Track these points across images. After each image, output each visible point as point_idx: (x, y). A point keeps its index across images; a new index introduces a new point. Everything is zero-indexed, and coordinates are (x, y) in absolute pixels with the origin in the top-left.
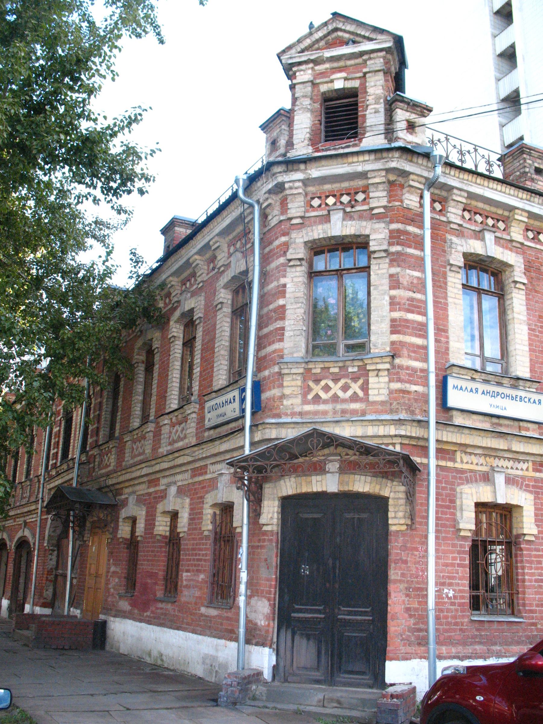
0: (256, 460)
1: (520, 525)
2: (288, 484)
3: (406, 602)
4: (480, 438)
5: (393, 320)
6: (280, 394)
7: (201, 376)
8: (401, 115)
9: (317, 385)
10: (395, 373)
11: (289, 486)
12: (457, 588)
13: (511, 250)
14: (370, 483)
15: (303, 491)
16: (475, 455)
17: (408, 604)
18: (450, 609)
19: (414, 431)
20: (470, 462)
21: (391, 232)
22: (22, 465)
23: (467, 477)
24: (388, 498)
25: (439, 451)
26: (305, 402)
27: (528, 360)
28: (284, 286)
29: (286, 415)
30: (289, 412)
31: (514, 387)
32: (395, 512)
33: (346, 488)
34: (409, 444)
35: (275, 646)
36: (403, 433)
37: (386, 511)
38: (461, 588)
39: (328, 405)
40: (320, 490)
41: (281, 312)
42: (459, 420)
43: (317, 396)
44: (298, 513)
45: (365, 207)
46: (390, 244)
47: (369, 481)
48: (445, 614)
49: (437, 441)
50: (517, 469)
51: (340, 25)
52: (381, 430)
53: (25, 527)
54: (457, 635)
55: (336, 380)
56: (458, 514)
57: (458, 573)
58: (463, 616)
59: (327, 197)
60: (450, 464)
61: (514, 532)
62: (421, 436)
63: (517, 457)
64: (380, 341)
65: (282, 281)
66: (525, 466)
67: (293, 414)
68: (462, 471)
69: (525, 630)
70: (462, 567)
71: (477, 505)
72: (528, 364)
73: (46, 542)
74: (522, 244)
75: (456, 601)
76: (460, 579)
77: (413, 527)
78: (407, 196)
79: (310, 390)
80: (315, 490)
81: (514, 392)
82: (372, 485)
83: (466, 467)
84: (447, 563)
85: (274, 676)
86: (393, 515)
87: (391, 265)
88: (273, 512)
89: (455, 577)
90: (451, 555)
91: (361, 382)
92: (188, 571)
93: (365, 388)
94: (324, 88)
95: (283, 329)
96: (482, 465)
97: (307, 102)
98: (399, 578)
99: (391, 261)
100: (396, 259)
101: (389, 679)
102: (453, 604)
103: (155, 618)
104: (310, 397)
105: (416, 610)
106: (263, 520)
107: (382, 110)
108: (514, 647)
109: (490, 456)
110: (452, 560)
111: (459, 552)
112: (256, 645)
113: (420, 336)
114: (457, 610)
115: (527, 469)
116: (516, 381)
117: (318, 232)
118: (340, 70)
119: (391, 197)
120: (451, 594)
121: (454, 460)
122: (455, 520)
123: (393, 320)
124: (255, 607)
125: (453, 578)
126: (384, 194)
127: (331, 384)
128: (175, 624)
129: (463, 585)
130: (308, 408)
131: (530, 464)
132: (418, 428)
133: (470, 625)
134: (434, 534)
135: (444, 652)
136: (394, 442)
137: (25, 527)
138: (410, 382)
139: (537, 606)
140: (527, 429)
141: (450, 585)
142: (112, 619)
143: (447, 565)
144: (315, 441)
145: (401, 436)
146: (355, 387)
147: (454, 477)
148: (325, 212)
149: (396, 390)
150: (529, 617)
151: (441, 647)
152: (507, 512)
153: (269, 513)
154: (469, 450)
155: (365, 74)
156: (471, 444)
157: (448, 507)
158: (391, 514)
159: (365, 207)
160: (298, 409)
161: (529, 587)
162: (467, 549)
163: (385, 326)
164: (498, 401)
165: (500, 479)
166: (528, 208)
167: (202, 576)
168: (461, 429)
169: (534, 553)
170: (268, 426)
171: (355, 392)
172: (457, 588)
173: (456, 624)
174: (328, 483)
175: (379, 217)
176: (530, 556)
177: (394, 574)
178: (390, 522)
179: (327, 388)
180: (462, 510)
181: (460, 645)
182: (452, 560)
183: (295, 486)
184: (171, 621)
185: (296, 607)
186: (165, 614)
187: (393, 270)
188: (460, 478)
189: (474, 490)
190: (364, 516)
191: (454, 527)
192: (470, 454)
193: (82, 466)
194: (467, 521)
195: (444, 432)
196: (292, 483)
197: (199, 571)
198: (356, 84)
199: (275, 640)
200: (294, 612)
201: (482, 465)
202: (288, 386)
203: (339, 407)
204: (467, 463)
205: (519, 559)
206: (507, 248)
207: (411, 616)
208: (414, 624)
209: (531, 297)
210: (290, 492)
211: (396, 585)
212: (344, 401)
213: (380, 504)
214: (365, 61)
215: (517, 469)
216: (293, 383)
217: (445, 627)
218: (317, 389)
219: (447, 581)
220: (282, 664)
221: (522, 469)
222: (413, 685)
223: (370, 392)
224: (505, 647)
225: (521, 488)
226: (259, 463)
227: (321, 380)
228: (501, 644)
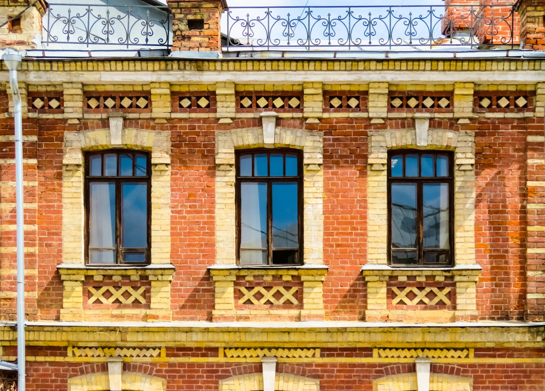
13: (153, 128)
20: (84, 354)
27: (169, 244)
50: (145, 356)
66: (155, 353)
68: (79, 364)
72: (169, 249)
74: (169, 120)
83: (77, 360)
96: (99, 356)
147: (67, 370)
192: (85, 348)
201: (99, 356)
204: (81, 356)
206: (147, 127)
209: (178, 176)
221: (151, 356)
225: (150, 374)
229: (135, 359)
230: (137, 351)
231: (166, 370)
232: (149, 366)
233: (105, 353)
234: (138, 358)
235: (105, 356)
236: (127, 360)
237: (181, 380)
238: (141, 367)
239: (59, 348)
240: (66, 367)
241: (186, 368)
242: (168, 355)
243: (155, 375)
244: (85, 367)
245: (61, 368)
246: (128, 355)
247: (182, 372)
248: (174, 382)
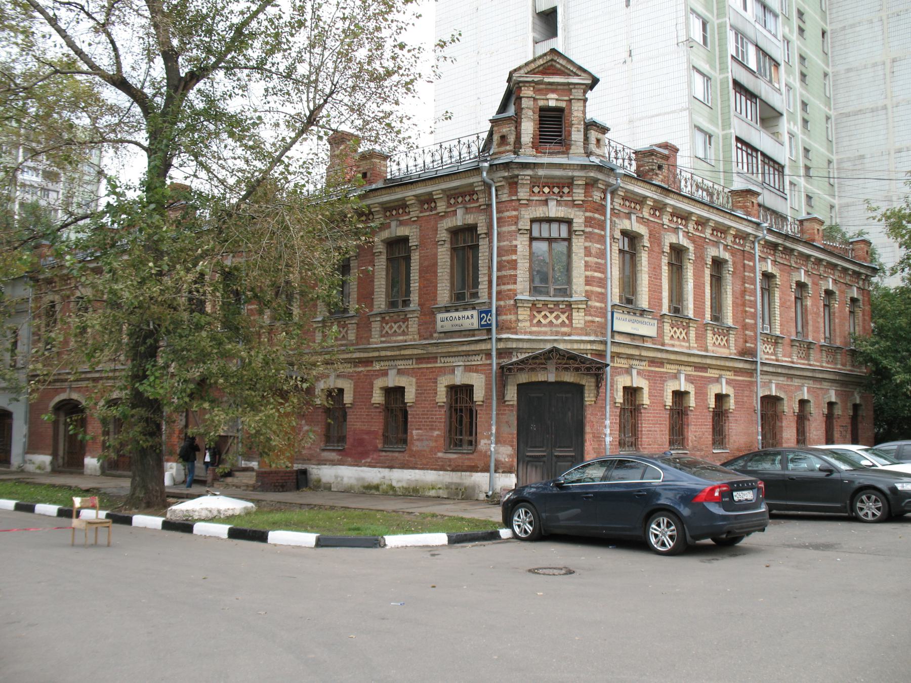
5: (586, 277)
7: (420, 289)
8: (593, 135)
10: (587, 311)
11: (523, 378)
21: (586, 218)
26: (532, 325)
28: (516, 246)
29: (521, 333)
31: (641, 315)
33: (559, 379)
41: (514, 265)
45: (570, 199)
46: (586, 226)
51: (556, 58)
52: (582, 346)
55: (551, 313)
59: (544, 187)
61: (637, 403)
63: (641, 359)
64: (579, 290)
65: (514, 243)
67: (525, 333)
71: (624, 388)
78: (595, 193)
79: (535, 317)
81: (640, 319)
87: (586, 241)
91: (566, 314)
92: (417, 429)
93: (570, 318)
94: (541, 103)
95: (516, 276)
97: (530, 113)
99: (586, 237)
100: (589, 236)
104: (535, 321)
106: (506, 399)
107: (582, 130)
113: (600, 287)
116: (643, 312)
117: (540, 212)
118: (553, 91)
119: (587, 194)
123: (586, 277)
126: (583, 191)
127: (548, 314)
128: (404, 466)
130: (535, 329)
138: (595, 316)
146: (563, 317)
148: (543, 198)
155: (570, 100)
158: (586, 395)
159: (570, 199)
160: (528, 330)
163: (582, 280)
164: (636, 325)
166: (655, 197)
167: (436, 433)
175: (578, 206)
177: (588, 429)
187: (587, 244)
190: (569, 395)
197: (432, 429)
198: (563, 104)
203: (554, 329)
210: (524, 381)
212: (556, 326)
213: (579, 389)
214: (571, 90)
218: (539, 317)
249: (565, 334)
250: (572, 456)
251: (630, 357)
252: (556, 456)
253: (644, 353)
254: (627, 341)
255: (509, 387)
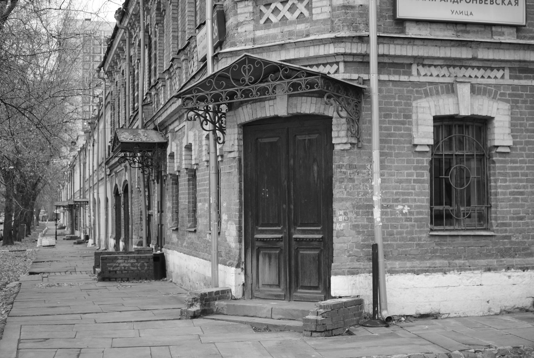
0: (199, 91)
1: (493, 138)
2: (245, 110)
3: (353, 220)
4: (437, 48)
6: (236, 23)
9: (268, 9)
11: (246, 114)
12: (413, 204)
14: (316, 104)
15: (258, 117)
16: (435, 66)
17: (356, 221)
18: (405, 225)
19: (357, 48)
20: (429, 74)
22: (122, 110)
23: (425, 91)
24: (331, 118)
25: (381, 66)
26: (256, 28)
30: (242, 39)
32: (338, 131)
33: (294, 111)
34: (353, 62)
35: (243, 267)
36: (342, 51)
37: (331, 130)
38: (418, 204)
39: (276, 29)
40: (272, 114)
42: (412, 31)
43: (268, 19)
44: (257, 139)
47: (315, 102)
48: (399, 230)
49: (379, 56)
50: (489, 77)
53: (126, 171)
54: (414, 250)
56: (414, 129)
57: (414, 189)
58: (421, 232)
60: (404, 78)
61: (489, 144)
62: (363, 52)
63: (488, 65)
66: (499, 74)
67: (245, 42)
69: (496, 244)
70: (419, 183)
71: (436, 119)
73: (137, 183)
75: (412, 217)
76: (417, 195)
77: (360, 145)
80: (268, 115)
82: (318, 106)
83: (423, 79)
84: (401, 180)
85: (243, 295)
86: (336, 135)
88: (235, 139)
89: (411, 193)
90: (406, 171)
98: (345, 196)
101: (334, 292)
102: (407, 220)
103: (188, 248)
104: (262, 22)
105: (364, 226)
108: (482, 261)
109: (454, 67)
110: (407, 176)
111: (415, 168)
112: (229, 266)
114: (413, 226)
115: (503, 77)
120: (406, 210)
121: (410, 74)
122: (411, 136)
124: (231, 231)
125: (409, 194)
127: (280, 6)
129: (422, 201)
130: (259, 33)
131: (507, 72)
132: (359, 44)
133: (429, 239)
134: (378, 151)
135: (398, 266)
136: (337, 60)
137: (126, 171)
139: (512, 218)
140: (502, 34)
141: (405, 201)
142: (168, 250)
143: (401, 182)
144: (247, 67)
145: (344, 54)
149: (338, 7)
150: (501, 230)
151: (394, 262)
152: (483, 124)
153: (230, 140)
154: (426, 62)
156: (426, 55)
157: (403, 123)
158: (334, 134)
160: (251, 36)
161: (502, 201)
162: (426, 164)
165: (464, 90)
168: (412, 41)
169: (509, 165)
170: (223, 55)
171: (301, 13)
172: (413, 204)
173: (412, 239)
174: (278, 107)
176: (504, 168)
177: (337, 192)
178: (333, 142)
179: (276, 11)
180: (417, 125)
181: (417, 259)
182: (407, 176)
183: (251, 112)
184: (195, 249)
185: (260, 228)
186: (193, 243)
188: (417, 92)
189: (432, 104)
190: (314, 137)
191: (410, 142)
192: (430, 66)
193: (145, 107)
194: (424, 134)
195: (392, 46)
196: (248, 109)
199: (243, 260)
200: (258, 233)
202: (241, 14)
203: (286, 29)
204: (425, 75)
205: (492, 172)
207: (359, 233)
208: (363, 241)
211: (341, 204)
212: (292, 23)
215: (489, 77)
216: (247, 10)
217: (399, 242)
218: (268, 13)
219: (401, 197)
220: (250, 282)
221: (496, 77)
222: (361, 298)
223: (314, 11)
224: (471, 261)
226: (201, 94)
227: (271, 4)
228: (466, 258)
229: (480, 81)
230: (482, 72)
231: (509, 94)
232: (493, 88)
233: (450, 73)
234: (482, 79)
235: (449, 76)
236: (474, 81)
237: (524, 105)
238: (485, 90)
239: (402, 65)
240: (410, 88)
241: (528, 93)
242: (511, 77)
243: (499, 99)
244: (430, 89)
245: (405, 89)
246: (473, 76)
247: (525, 97)
248: (517, 107)
249: (300, 34)
250: (319, 240)
251: (451, 63)
252: (296, 239)
253: (483, 54)
254: (448, 34)
255: (227, 131)
